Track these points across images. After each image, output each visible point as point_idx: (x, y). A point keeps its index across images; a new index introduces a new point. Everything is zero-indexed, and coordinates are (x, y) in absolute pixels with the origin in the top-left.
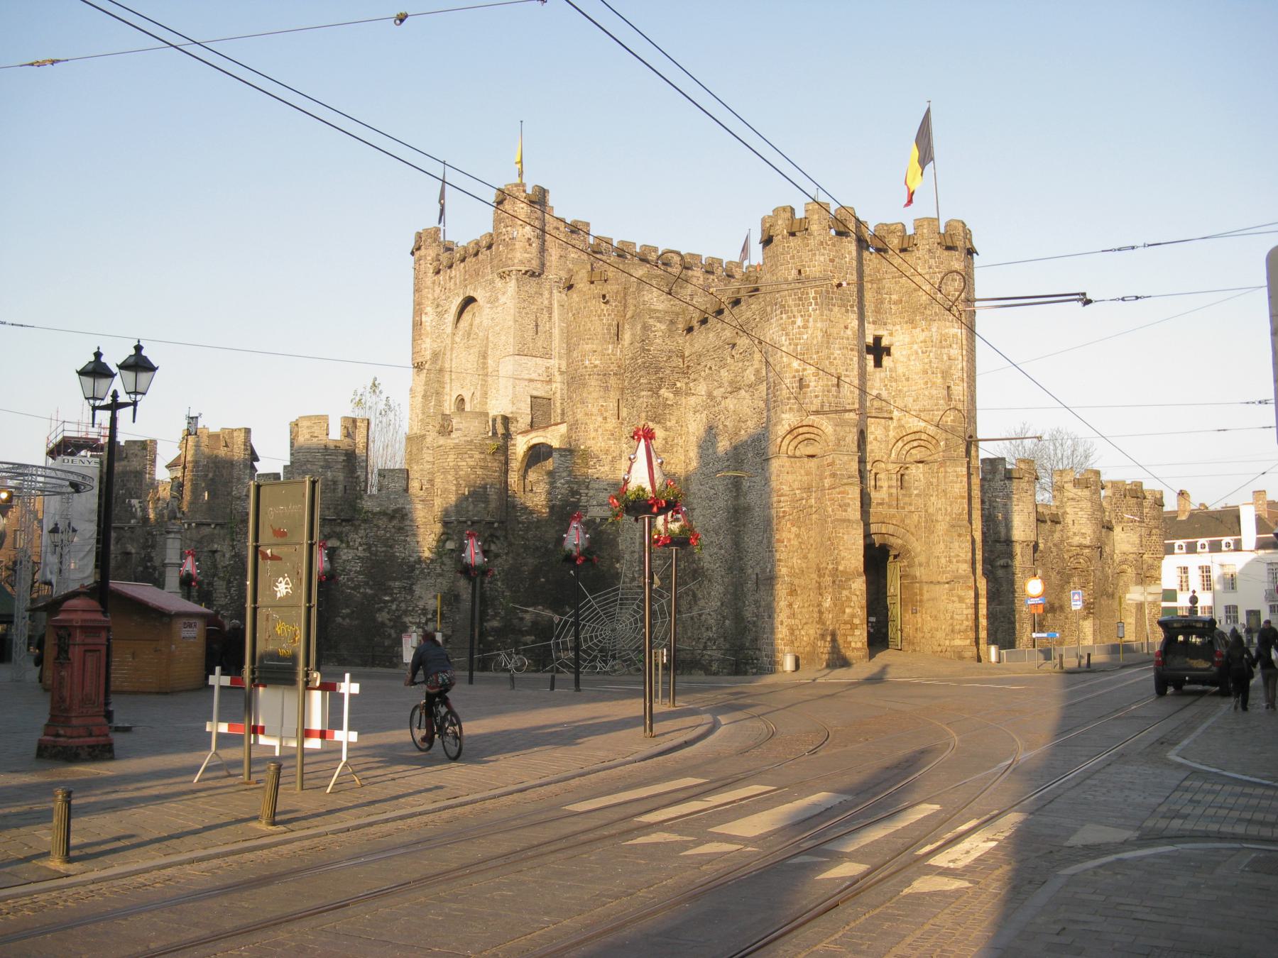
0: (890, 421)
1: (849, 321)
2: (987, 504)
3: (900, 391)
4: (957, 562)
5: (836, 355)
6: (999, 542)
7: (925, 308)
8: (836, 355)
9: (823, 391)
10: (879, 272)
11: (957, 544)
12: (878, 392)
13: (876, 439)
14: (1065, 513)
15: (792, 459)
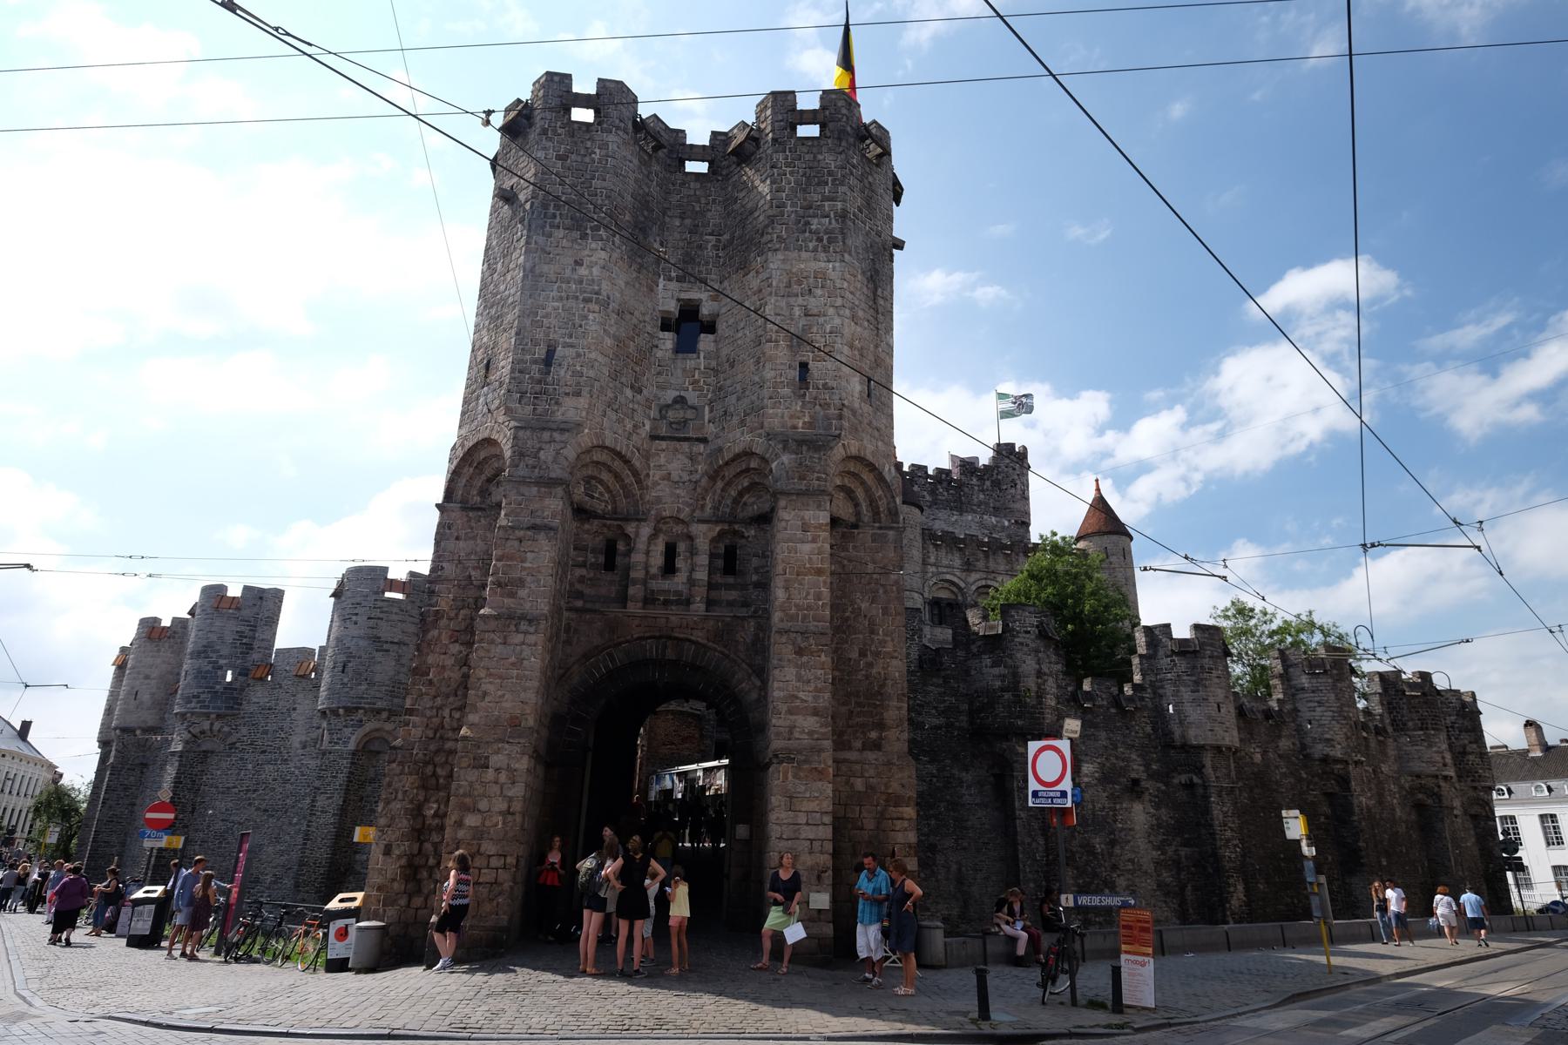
0: (702, 446)
1: (587, 252)
2: (1149, 690)
3: (720, 389)
4: (790, 712)
5: (549, 310)
6: (1174, 747)
7: (762, 235)
8: (549, 310)
9: (513, 371)
10: (699, 202)
11: (790, 673)
12: (677, 393)
13: (668, 477)
14: (1296, 710)
15: (471, 514)
